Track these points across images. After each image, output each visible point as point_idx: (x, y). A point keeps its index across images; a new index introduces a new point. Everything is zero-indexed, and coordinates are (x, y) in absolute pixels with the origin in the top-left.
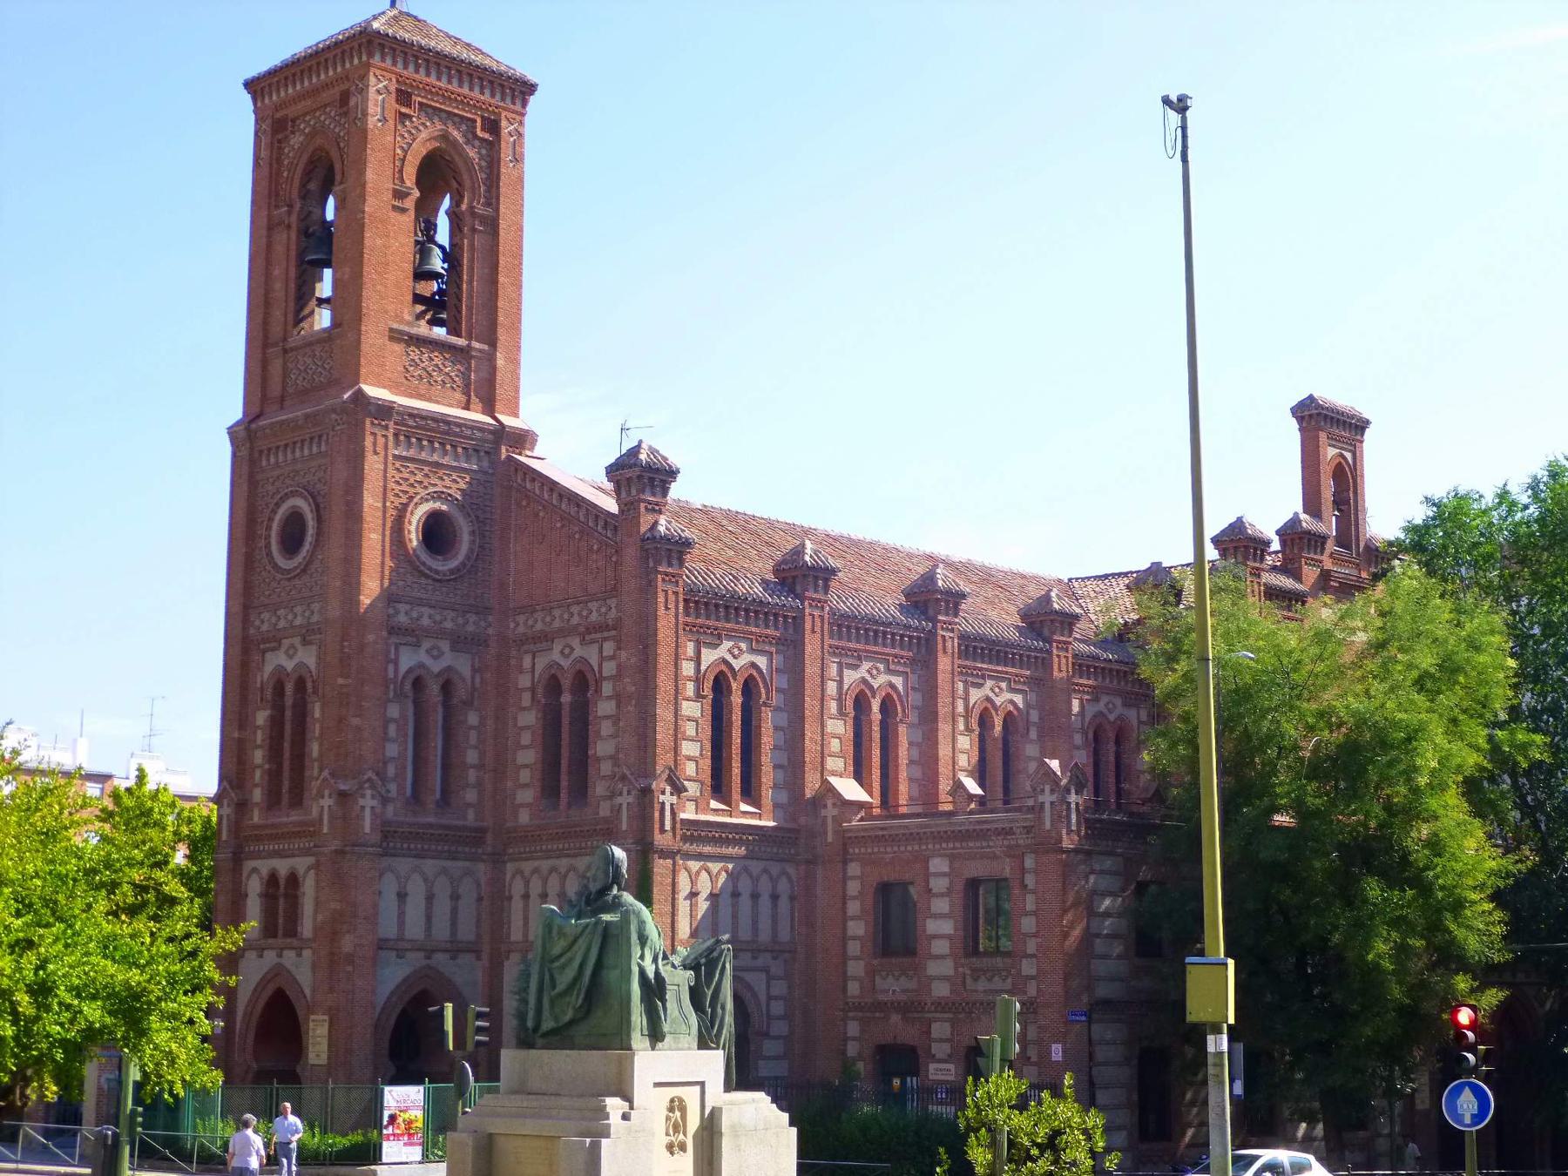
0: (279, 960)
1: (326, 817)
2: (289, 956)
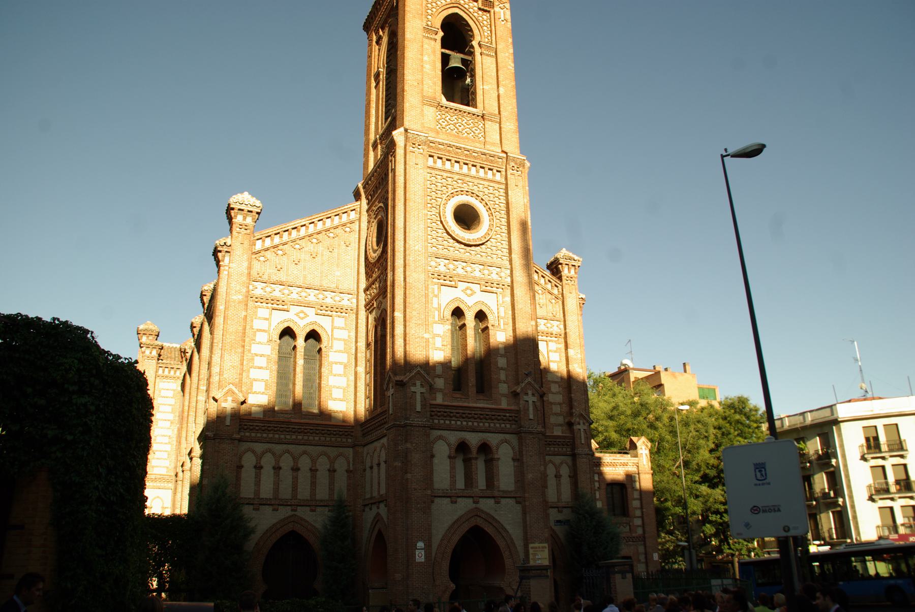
0: (474, 505)
1: (531, 409)
2: (487, 505)
